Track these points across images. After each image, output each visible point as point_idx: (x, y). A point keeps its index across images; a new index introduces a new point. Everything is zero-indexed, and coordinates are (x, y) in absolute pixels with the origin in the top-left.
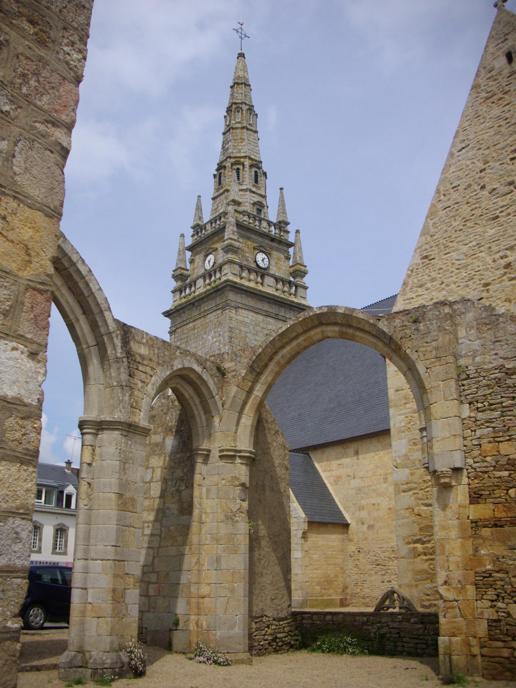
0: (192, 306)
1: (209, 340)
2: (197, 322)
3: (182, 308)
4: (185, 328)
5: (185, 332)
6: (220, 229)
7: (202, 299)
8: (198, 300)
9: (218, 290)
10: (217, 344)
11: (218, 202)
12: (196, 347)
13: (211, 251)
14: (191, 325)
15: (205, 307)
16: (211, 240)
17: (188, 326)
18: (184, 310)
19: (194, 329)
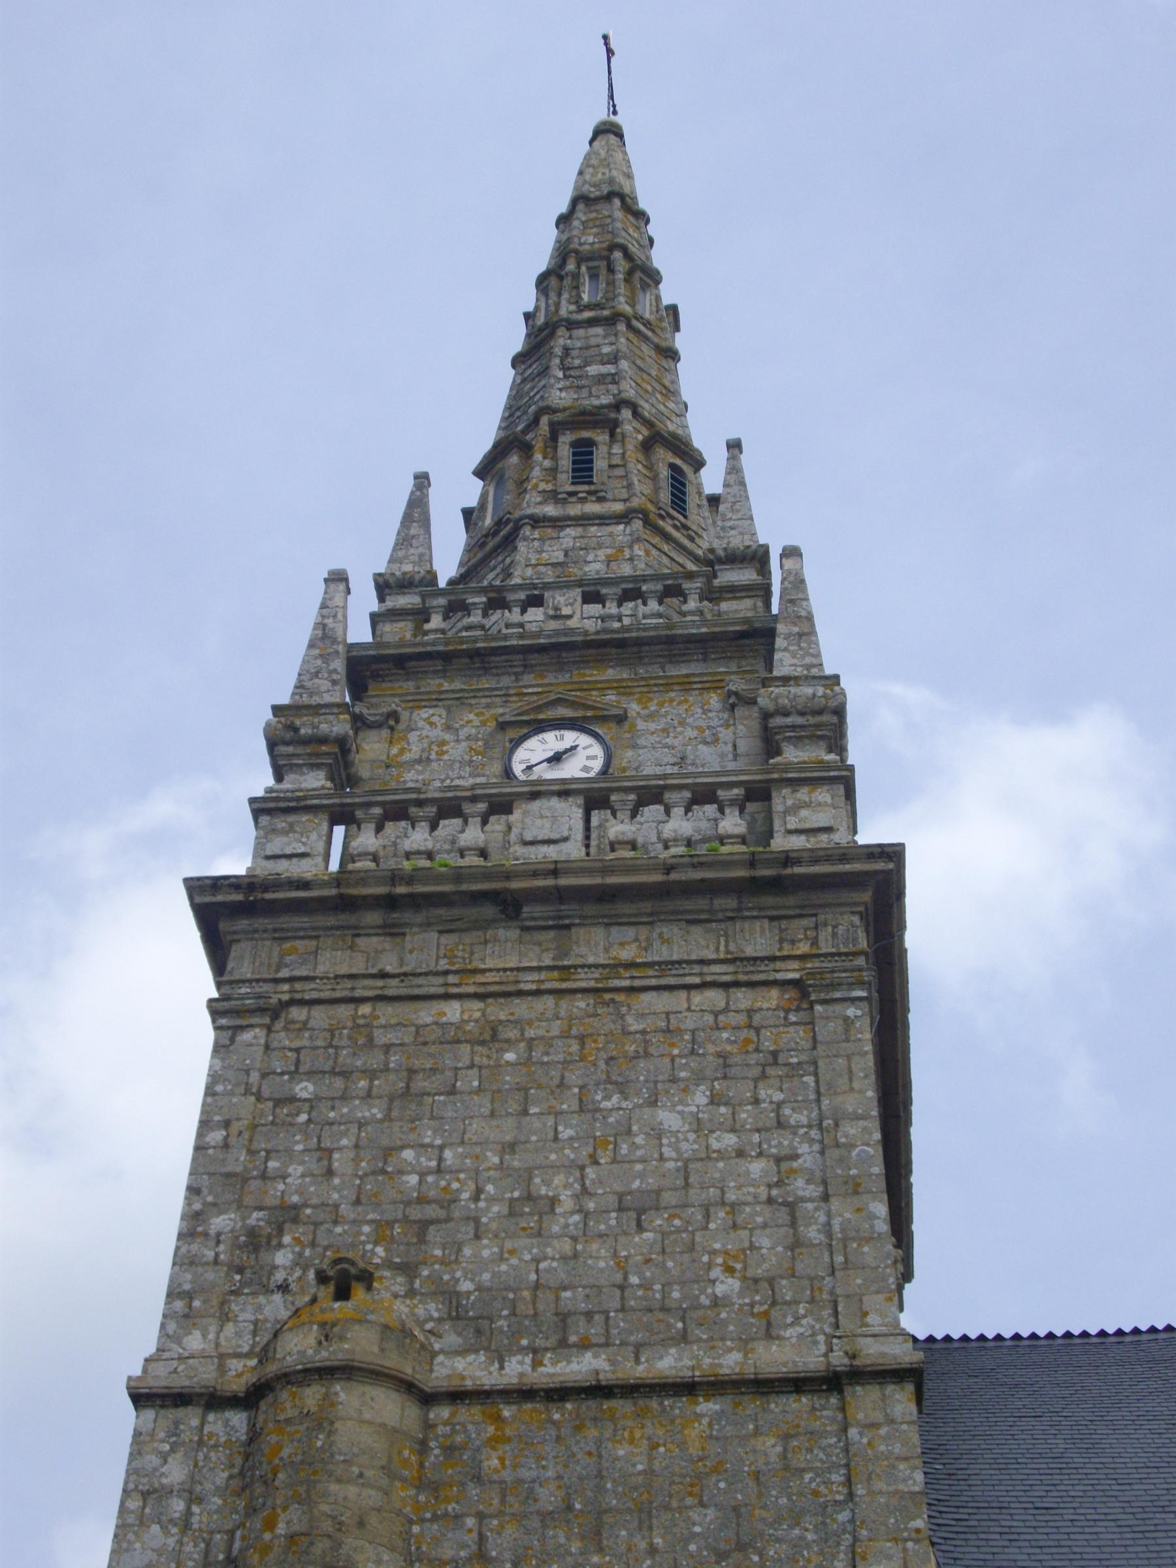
0: (489, 911)
1: (657, 1134)
2: (521, 1008)
3: (391, 903)
4: (387, 1013)
5: (381, 1038)
6: (670, 641)
7: (606, 895)
8: (561, 895)
9: (776, 885)
10: (757, 1168)
11: (567, 542)
12: (511, 1147)
13: (563, 712)
14: (453, 1011)
15: (596, 946)
16: (561, 667)
17: (425, 1014)
18: (408, 916)
19: (491, 1036)
